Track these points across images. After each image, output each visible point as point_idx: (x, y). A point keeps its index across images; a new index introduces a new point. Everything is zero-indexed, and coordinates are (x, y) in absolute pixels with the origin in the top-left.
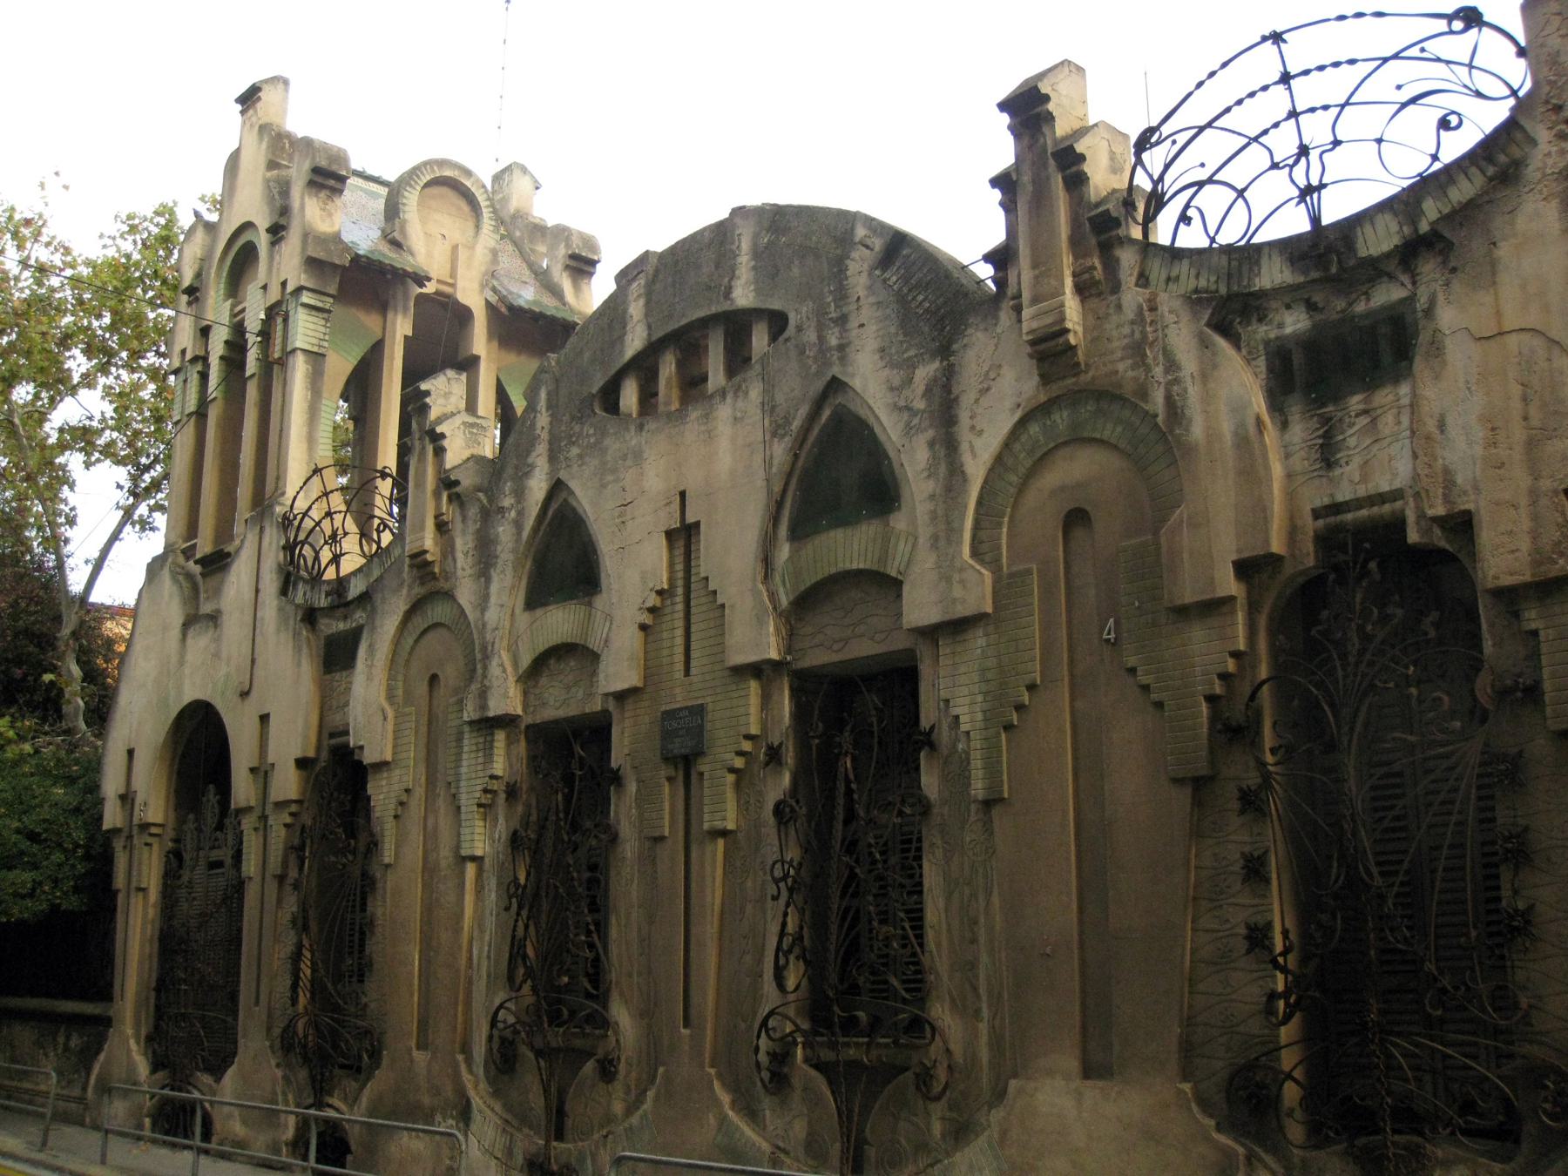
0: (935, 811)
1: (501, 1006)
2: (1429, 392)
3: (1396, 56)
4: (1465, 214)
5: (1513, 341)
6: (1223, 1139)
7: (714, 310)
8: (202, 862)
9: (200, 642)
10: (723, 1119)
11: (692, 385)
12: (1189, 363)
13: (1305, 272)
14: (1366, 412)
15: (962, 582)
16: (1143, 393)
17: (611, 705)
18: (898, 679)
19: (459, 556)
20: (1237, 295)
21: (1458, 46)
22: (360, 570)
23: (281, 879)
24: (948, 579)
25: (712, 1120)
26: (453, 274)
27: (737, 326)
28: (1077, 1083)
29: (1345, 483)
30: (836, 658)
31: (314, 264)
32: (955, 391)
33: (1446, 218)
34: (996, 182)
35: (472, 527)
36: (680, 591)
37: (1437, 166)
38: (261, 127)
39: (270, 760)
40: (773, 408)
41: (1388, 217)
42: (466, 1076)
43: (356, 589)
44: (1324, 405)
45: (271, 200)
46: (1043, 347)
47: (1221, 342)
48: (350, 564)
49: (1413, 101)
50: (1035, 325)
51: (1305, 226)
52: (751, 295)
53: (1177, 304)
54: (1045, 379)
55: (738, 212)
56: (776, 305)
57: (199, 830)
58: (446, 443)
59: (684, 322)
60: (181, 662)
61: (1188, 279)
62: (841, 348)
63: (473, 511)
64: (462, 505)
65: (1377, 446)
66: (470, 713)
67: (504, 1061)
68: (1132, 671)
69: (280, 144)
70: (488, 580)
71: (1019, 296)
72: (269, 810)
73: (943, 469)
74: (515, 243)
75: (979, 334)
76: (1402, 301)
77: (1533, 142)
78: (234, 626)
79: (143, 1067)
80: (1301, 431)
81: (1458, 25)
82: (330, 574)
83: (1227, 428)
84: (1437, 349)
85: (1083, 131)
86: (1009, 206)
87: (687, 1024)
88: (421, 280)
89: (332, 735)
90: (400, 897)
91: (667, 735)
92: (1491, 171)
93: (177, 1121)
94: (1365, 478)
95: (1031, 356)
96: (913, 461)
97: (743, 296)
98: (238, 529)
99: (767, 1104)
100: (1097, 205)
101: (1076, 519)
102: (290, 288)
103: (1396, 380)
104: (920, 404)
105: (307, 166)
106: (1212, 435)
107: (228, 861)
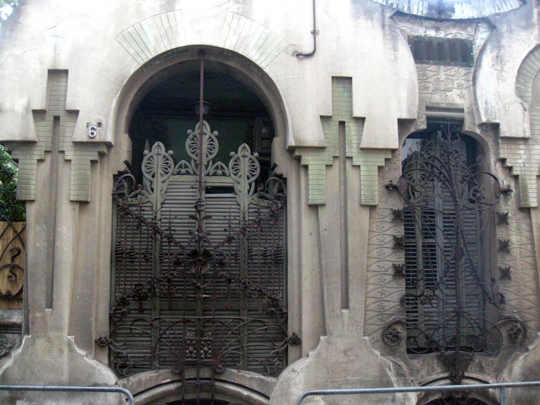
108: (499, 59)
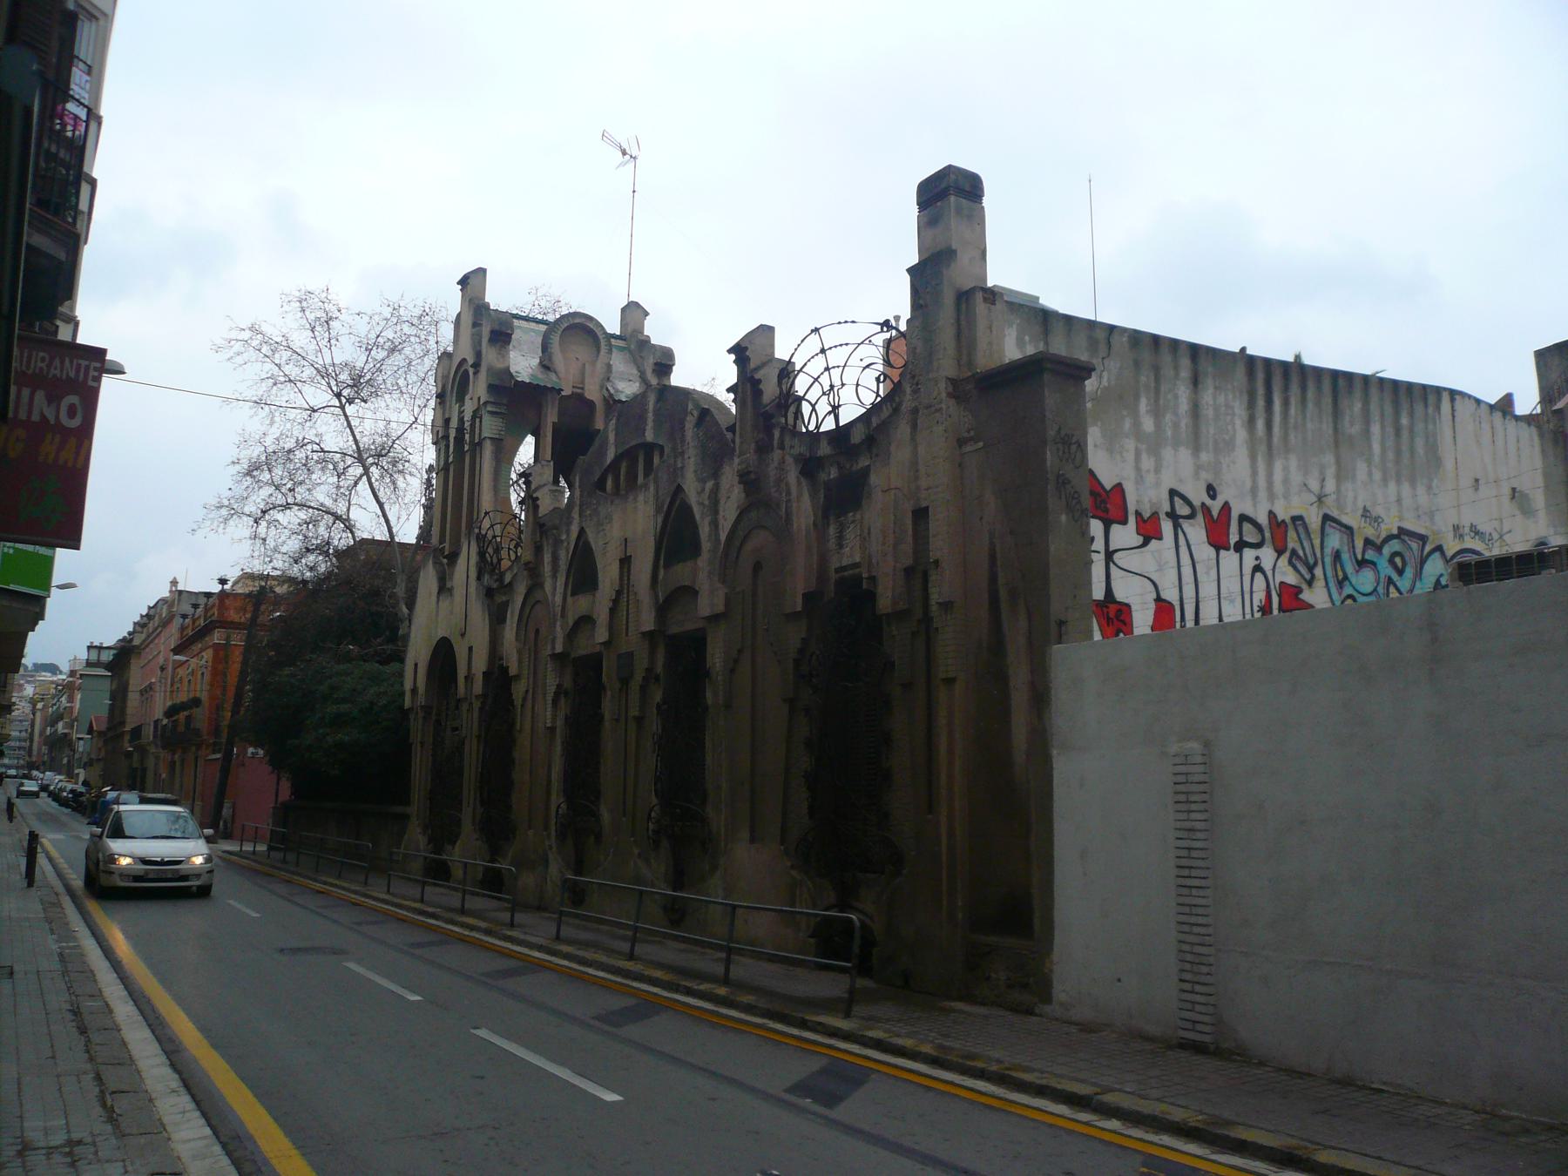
4: (884, 426)
6: (794, 873)
9: (445, 604)
11: (632, 477)
26: (583, 382)
27: (649, 449)
31: (492, 388)
48: (505, 564)
54: (748, 493)
66: (549, 652)
78: (459, 593)
79: (422, 840)
85: (764, 365)
93: (438, 872)
96: (704, 530)
97: (649, 436)
101: (757, 567)
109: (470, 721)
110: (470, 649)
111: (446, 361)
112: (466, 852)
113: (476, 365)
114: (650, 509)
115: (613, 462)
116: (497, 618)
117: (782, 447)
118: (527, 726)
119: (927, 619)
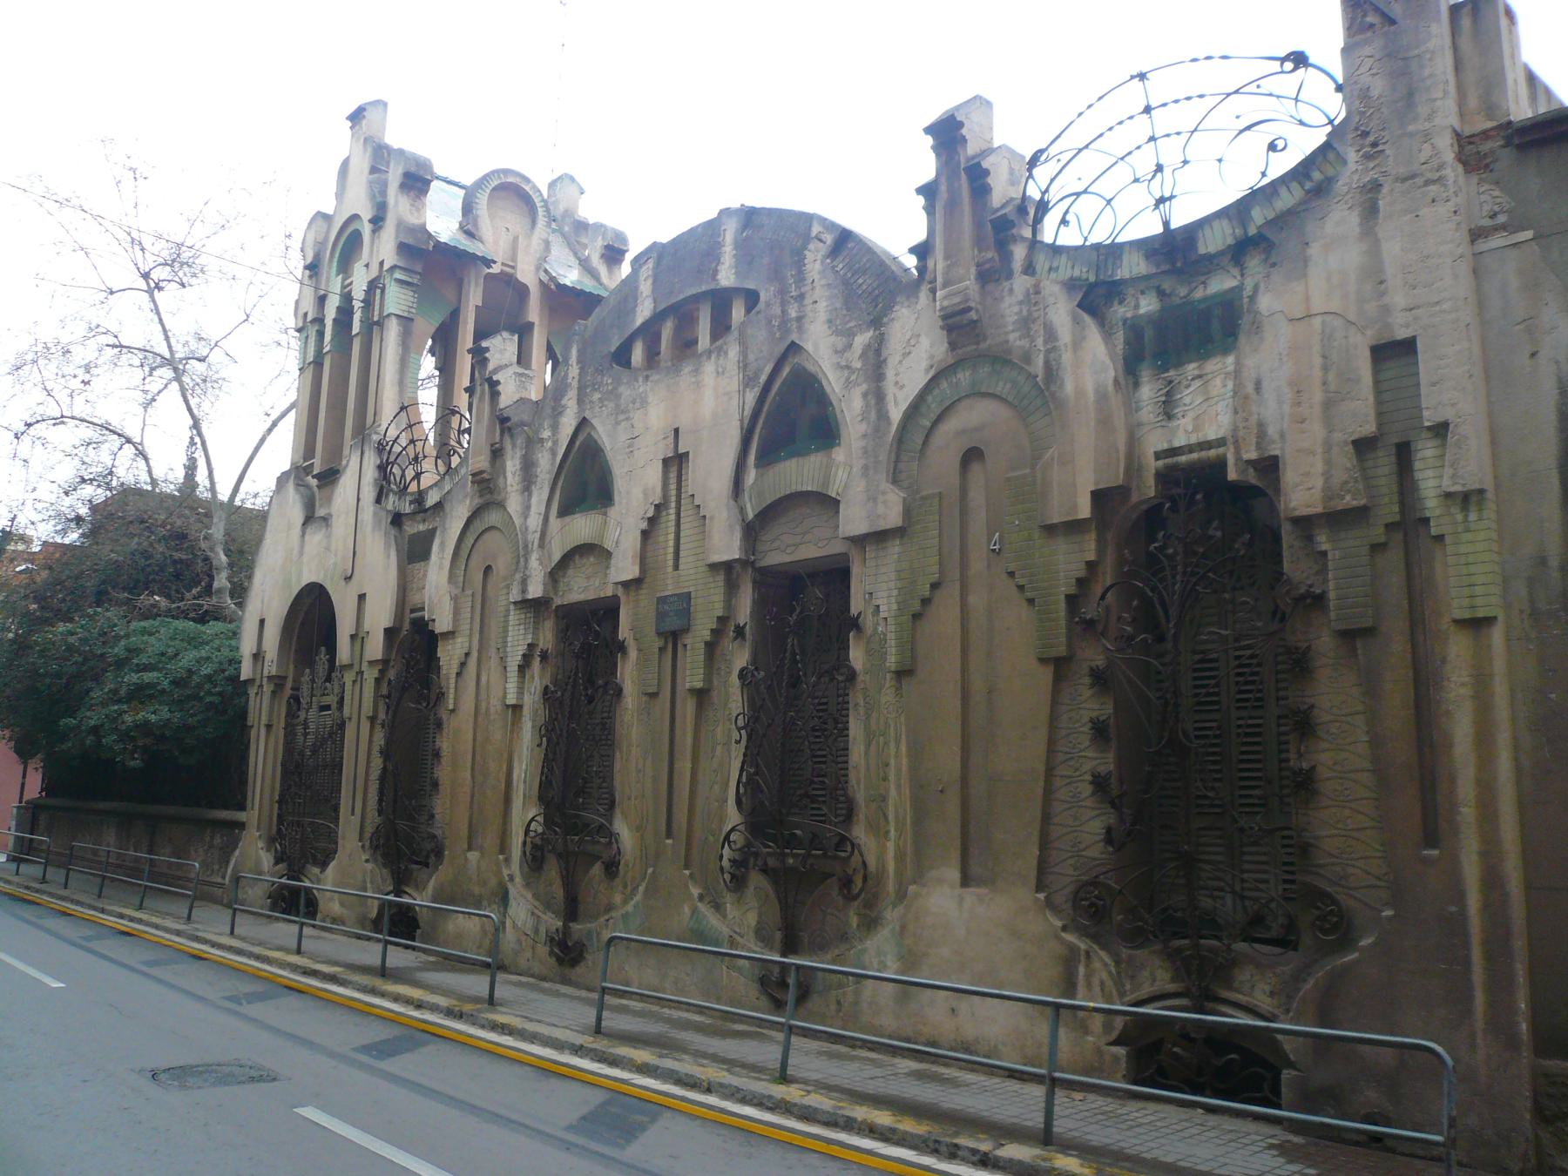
0: (860, 678)
1: (533, 819)
2: (1250, 362)
3: (1236, 92)
4: (1284, 220)
5: (1317, 321)
6: (1070, 937)
7: (704, 288)
8: (315, 706)
9: (315, 538)
10: (694, 910)
11: (685, 346)
12: (1065, 333)
13: (1158, 266)
14: (1200, 376)
15: (885, 502)
16: (1027, 358)
17: (620, 591)
18: (835, 575)
19: (509, 475)
20: (1104, 282)
21: (1289, 82)
22: (435, 484)
23: (373, 719)
24: (875, 500)
25: (687, 910)
26: (514, 257)
27: (721, 301)
28: (959, 891)
29: (1181, 432)
30: (788, 559)
31: (403, 248)
32: (885, 353)
33: (1269, 223)
34: (921, 191)
35: (519, 453)
36: (673, 505)
37: (1266, 181)
38: (366, 140)
39: (366, 627)
40: (746, 366)
41: (1225, 222)
42: (506, 872)
43: (432, 499)
44: (1167, 371)
45: (373, 197)
46: (950, 321)
47: (1087, 318)
48: (426, 480)
49: (1248, 128)
50: (946, 303)
51: (1159, 229)
52: (732, 278)
53: (1056, 288)
54: (953, 346)
55: (725, 213)
56: (751, 286)
57: (313, 681)
58: (500, 388)
59: (682, 297)
60: (301, 553)
61: (1066, 271)
62: (799, 319)
63: (520, 441)
64: (512, 436)
65: (1205, 406)
66: (515, 595)
67: (535, 859)
68: (1011, 574)
69: (380, 154)
70: (530, 495)
71: (934, 281)
72: (365, 667)
73: (873, 415)
74: (563, 235)
75: (904, 310)
76: (1233, 289)
77: (1345, 162)
78: (342, 525)
79: (267, 860)
80: (1148, 391)
81: (1289, 66)
82: (413, 487)
83: (1090, 388)
84: (1257, 327)
86: (930, 209)
87: (669, 834)
88: (488, 263)
89: (412, 611)
90: (457, 735)
91: (661, 616)
92: (1308, 185)
93: (293, 903)
94: (1196, 428)
95: (942, 328)
96: (850, 406)
98: (346, 452)
99: (728, 899)
100: (998, 210)
101: (972, 456)
102: (386, 267)
103: (1226, 351)
104: (858, 365)
105: (400, 171)
106: (1080, 393)
107: (334, 706)
108: (442, 544)
109: (361, 698)
110: (362, 597)
111: (320, 222)
112: (348, 875)
113: (377, 221)
114: (733, 382)
115: (646, 324)
116: (415, 552)
117: (1029, 269)
118: (468, 704)
119: (1411, 525)
